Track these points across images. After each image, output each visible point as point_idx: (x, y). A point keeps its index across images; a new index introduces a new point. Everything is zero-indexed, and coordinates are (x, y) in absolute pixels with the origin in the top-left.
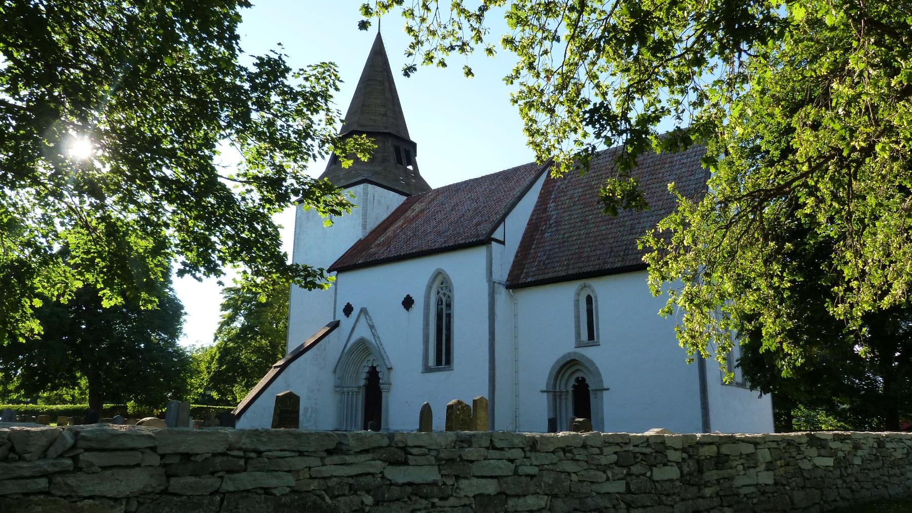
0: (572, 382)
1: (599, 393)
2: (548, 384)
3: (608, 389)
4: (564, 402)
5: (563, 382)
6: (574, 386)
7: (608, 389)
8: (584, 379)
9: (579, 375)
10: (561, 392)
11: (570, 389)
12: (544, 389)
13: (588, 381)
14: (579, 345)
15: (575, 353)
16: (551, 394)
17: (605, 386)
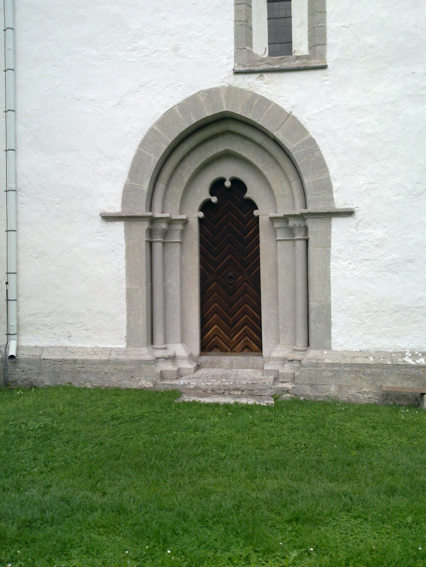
0: (202, 193)
1: (313, 226)
2: (128, 192)
3: (349, 213)
4: (176, 250)
5: (177, 190)
6: (206, 206)
7: (349, 213)
8: (239, 185)
9: (228, 171)
10: (170, 222)
11: (194, 215)
12: (116, 208)
13: (254, 191)
14: (247, 68)
15: (231, 91)
16: (146, 225)
17: (340, 204)
